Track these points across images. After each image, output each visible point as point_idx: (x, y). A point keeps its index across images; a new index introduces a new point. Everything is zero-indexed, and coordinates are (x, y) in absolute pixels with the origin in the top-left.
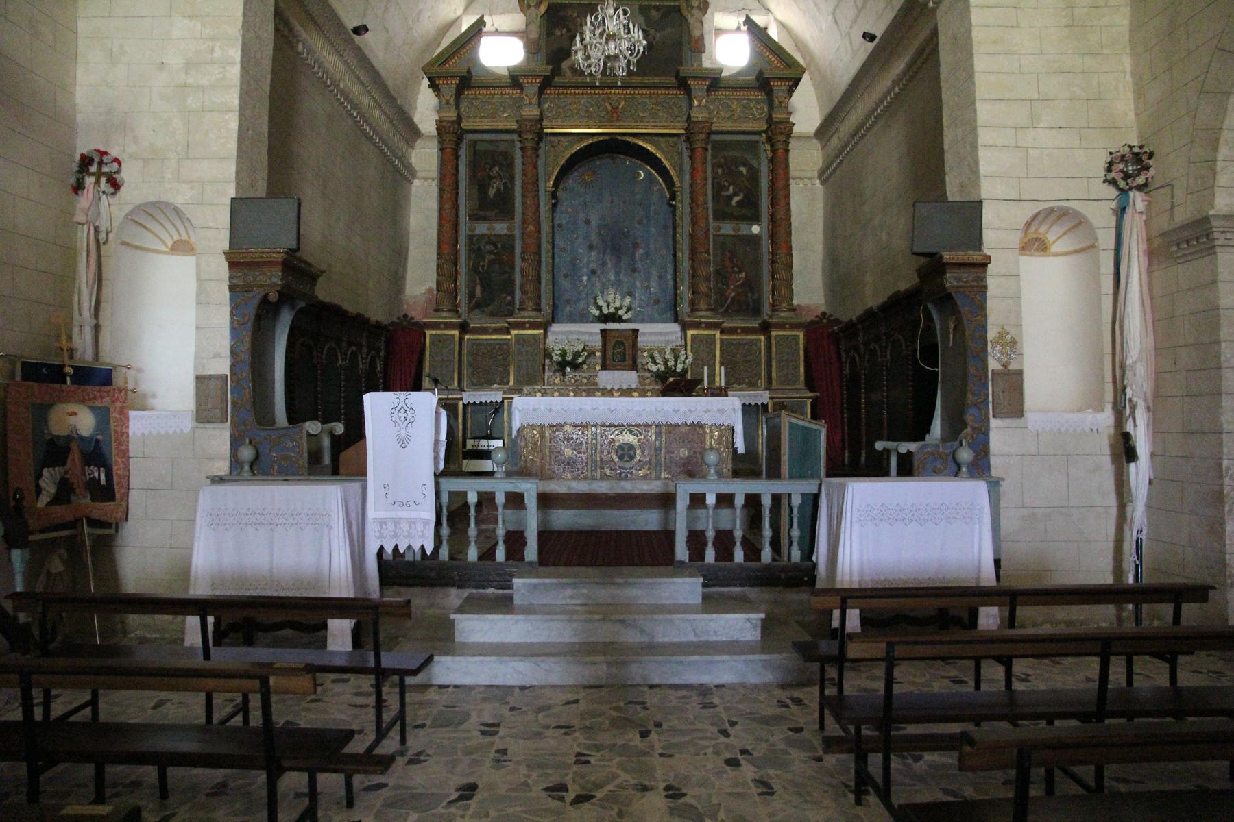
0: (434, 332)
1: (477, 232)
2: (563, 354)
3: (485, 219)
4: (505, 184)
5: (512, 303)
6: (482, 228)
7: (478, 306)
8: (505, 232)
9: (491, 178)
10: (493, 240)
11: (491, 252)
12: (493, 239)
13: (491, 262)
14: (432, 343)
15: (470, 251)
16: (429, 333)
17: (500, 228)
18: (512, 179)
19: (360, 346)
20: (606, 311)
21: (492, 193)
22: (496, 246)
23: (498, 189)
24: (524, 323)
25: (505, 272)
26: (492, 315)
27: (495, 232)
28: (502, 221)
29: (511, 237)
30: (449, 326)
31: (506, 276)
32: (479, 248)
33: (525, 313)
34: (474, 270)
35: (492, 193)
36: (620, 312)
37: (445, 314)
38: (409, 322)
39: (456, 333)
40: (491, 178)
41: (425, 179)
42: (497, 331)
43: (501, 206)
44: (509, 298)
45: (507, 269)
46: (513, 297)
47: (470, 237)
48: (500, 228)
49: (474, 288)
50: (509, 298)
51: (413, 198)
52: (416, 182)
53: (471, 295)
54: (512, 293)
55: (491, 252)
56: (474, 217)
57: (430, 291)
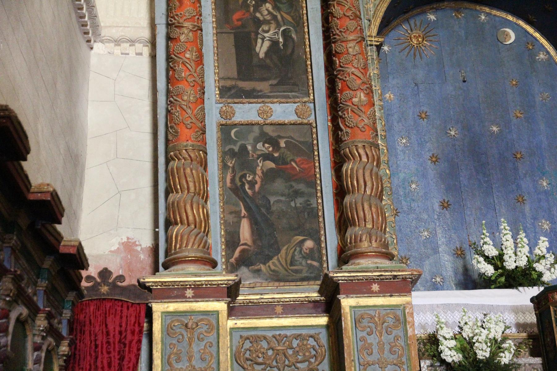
0: (172, 307)
1: (237, 118)
2: (467, 347)
3: (251, 95)
4: (285, 34)
5: (317, 254)
6: (246, 112)
7: (245, 261)
8: (293, 118)
9: (258, 23)
10: (270, 135)
11: (267, 157)
12: (268, 130)
13: (269, 176)
14: (168, 331)
15: (225, 155)
16: (159, 308)
17: (283, 112)
18: (300, 23)
19: (34, 310)
20: (510, 264)
21: (262, 48)
22: (274, 142)
23: (274, 43)
24: (370, 281)
25: (297, 194)
26: (277, 278)
27: (274, 118)
28: (286, 99)
29: (310, 128)
30: (202, 292)
31: (299, 201)
32: (243, 148)
33: (364, 263)
34: (235, 191)
35: (262, 48)
36: (539, 267)
37: (192, 268)
38: (114, 286)
39: (221, 306)
40: (258, 23)
41: (117, 42)
42: (291, 309)
43: (284, 71)
44: (309, 244)
45: (301, 187)
46: (318, 241)
47: (225, 129)
48: (283, 112)
49: (238, 224)
50: (309, 244)
51: (92, 75)
52: (98, 47)
53: (232, 240)
54: (316, 235)
55: (267, 157)
56: (226, 92)
57: (129, 246)
